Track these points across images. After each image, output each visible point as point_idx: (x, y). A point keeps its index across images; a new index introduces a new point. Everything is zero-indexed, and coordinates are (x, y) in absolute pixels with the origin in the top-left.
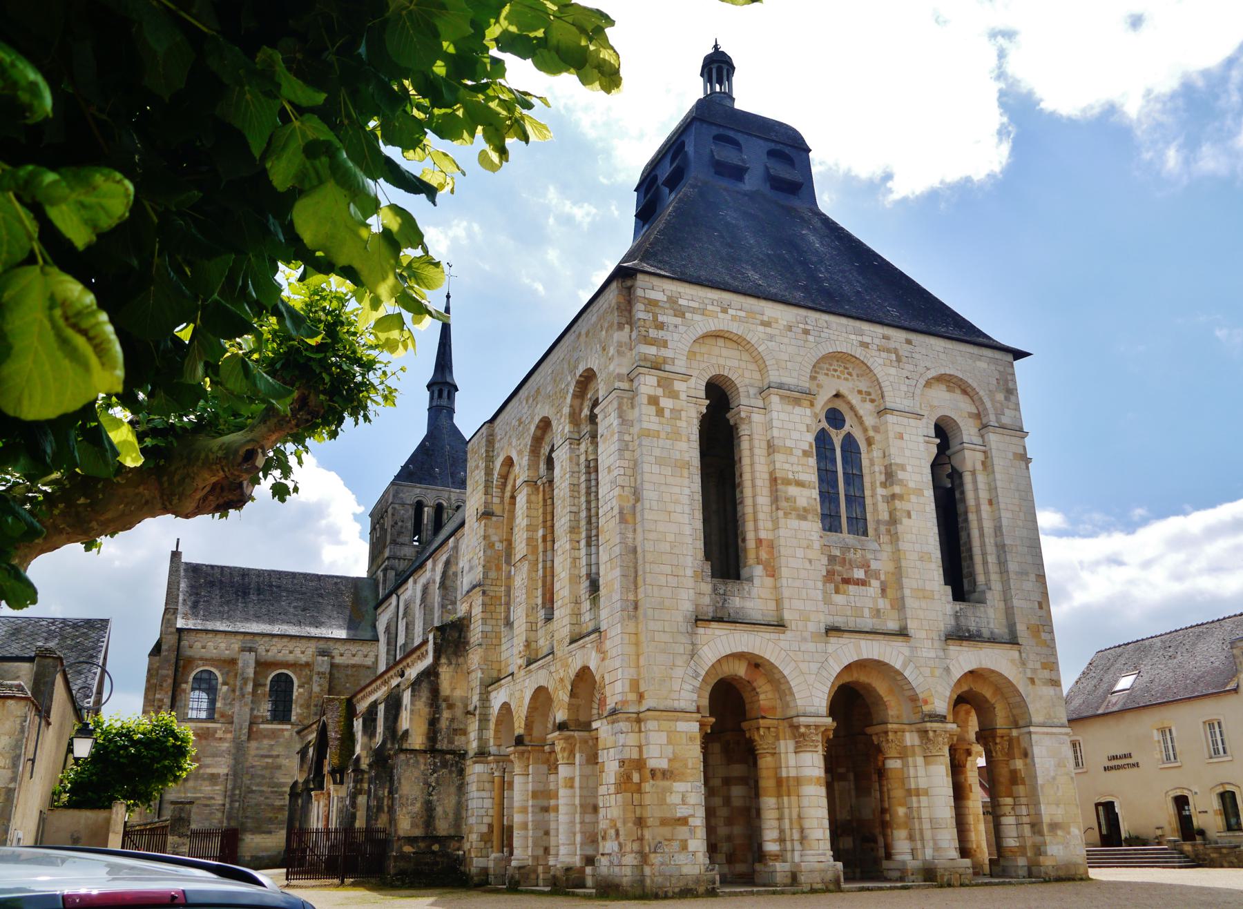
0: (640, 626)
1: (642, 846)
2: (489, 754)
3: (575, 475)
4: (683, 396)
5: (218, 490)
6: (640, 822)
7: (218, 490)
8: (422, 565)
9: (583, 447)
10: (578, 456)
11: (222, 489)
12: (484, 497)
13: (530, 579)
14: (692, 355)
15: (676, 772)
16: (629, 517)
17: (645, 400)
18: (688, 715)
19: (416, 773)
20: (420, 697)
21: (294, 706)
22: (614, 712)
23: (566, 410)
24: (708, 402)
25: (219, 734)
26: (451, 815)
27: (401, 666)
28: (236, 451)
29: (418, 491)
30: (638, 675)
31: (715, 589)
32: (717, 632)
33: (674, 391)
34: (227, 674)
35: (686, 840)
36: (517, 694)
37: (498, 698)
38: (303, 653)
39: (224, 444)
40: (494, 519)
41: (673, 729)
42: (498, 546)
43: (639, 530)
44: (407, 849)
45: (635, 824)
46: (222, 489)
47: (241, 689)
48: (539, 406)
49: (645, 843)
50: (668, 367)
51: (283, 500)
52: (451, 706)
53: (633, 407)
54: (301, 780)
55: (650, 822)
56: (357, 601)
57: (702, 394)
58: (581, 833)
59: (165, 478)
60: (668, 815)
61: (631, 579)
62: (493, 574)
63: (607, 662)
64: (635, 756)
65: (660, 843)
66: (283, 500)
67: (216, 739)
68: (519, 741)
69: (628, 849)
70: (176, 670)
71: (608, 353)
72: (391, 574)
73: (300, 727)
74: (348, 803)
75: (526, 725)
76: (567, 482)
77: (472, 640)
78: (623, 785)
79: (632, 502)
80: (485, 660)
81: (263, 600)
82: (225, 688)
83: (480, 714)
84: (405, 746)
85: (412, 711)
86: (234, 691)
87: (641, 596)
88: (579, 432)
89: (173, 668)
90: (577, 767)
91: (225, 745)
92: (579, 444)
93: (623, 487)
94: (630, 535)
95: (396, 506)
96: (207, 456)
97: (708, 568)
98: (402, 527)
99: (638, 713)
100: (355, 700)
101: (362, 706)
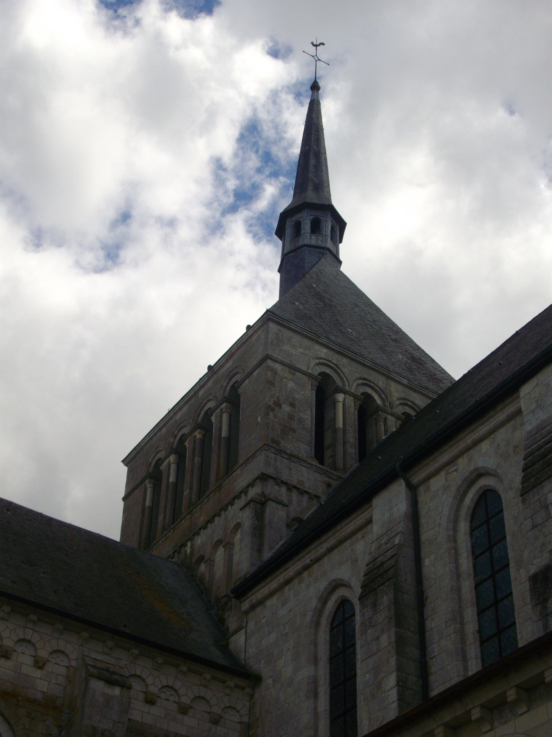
98: (291, 417)
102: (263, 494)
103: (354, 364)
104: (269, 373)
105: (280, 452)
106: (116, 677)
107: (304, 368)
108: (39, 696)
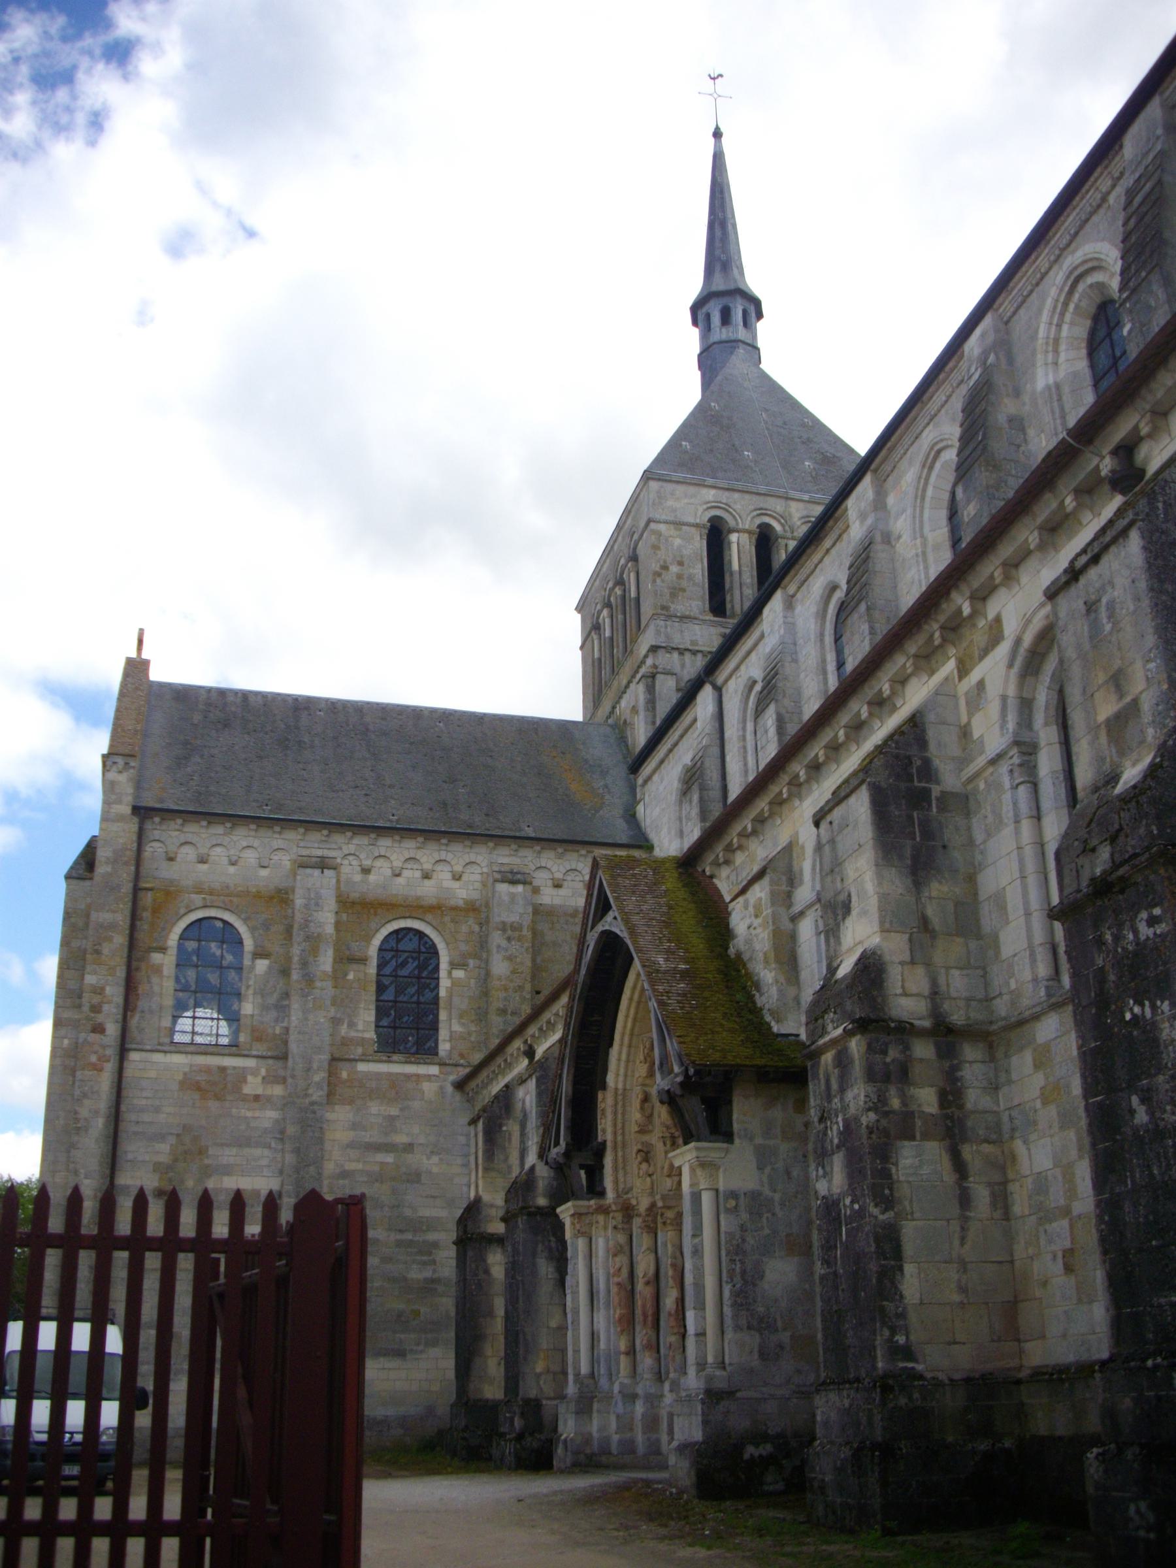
21: (443, 1016)
25: (253, 1086)
34: (266, 926)
38: (457, 877)
47: (304, 964)
67: (245, 1098)
70: (134, 916)
73: (464, 1072)
82: (262, 965)
86: (285, 972)
89: (126, 907)
91: (268, 1117)
95: (662, 527)
98: (679, 577)
102: (655, 666)
103: (747, 496)
104: (653, 537)
105: (669, 617)
106: (519, 876)
107: (691, 520)
108: (461, 903)
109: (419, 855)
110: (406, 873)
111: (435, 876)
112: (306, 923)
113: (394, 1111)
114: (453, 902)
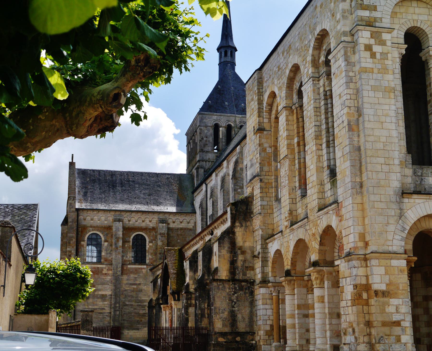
0: (364, 199)
1: (370, 338)
2: (269, 282)
3: (318, 101)
4: (389, 43)
5: (98, 120)
6: (369, 324)
7: (98, 120)
8: (220, 165)
9: (321, 82)
10: (319, 88)
11: (101, 120)
12: (258, 119)
13: (290, 170)
14: (394, 14)
15: (391, 292)
16: (355, 127)
17: (362, 48)
18: (399, 255)
19: (224, 294)
20: (224, 247)
21: (147, 254)
22: (349, 254)
23: (309, 58)
24: (406, 46)
25: (105, 271)
26: (247, 320)
27: (211, 228)
28: (108, 95)
29: (215, 117)
30: (365, 230)
31: (415, 173)
32: (417, 201)
33: (382, 40)
34: (107, 235)
35: (400, 336)
36: (285, 244)
37: (273, 247)
38: (150, 221)
39: (100, 91)
40: (265, 132)
41: (389, 264)
42: (269, 150)
43: (362, 135)
44: (221, 339)
45: (365, 325)
46: (101, 120)
47: (116, 244)
48: (291, 57)
49: (372, 337)
50: (377, 24)
51: (138, 124)
52: (243, 253)
53: (354, 53)
54: (154, 299)
55: (375, 324)
56: (181, 188)
57: (402, 41)
58: (330, 330)
59: (67, 115)
60: (387, 320)
61: (358, 168)
62: (266, 168)
63: (343, 222)
64: (364, 282)
65: (382, 337)
66: (138, 124)
67: (103, 274)
68: (288, 273)
69: (361, 340)
70: (77, 234)
71: (336, 18)
72: (201, 171)
73: (152, 267)
74: (183, 312)
75: (292, 263)
76: (312, 106)
77: (255, 211)
78: (356, 301)
79: (356, 117)
80: (264, 223)
81: (124, 190)
82: (106, 244)
83: (262, 257)
84: (216, 278)
85: (219, 256)
86: (111, 245)
87: (364, 178)
88: (318, 73)
89: (75, 232)
90: (326, 290)
92: (319, 81)
93: (350, 107)
94: (356, 139)
95: (202, 128)
96: (91, 99)
97: (409, 158)
98: (206, 141)
99: (365, 255)
100: (184, 250)
101: (189, 253)
106: (164, 222)
108: (151, 228)
109: (141, 217)
110: (138, 221)
111: (145, 221)
112: (116, 235)
113: (136, 276)
114: (149, 227)
